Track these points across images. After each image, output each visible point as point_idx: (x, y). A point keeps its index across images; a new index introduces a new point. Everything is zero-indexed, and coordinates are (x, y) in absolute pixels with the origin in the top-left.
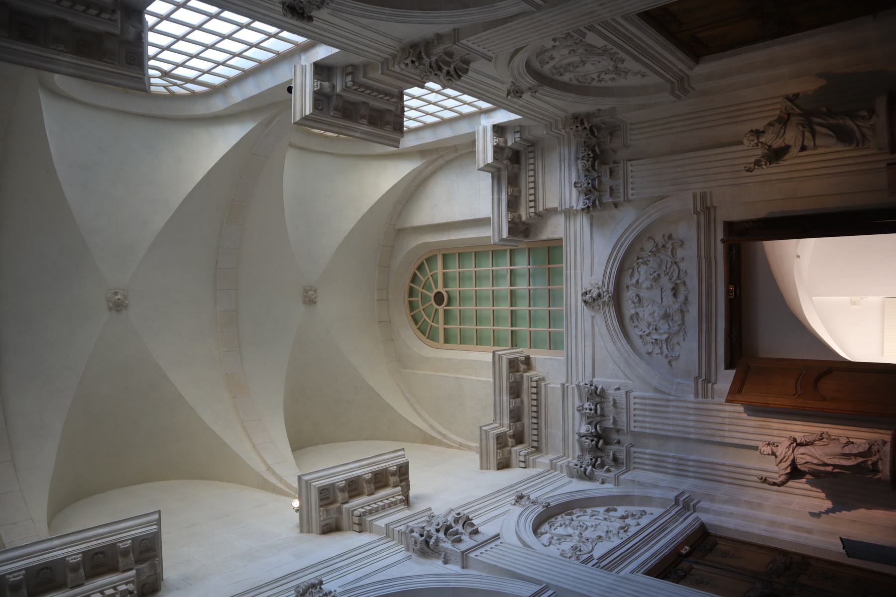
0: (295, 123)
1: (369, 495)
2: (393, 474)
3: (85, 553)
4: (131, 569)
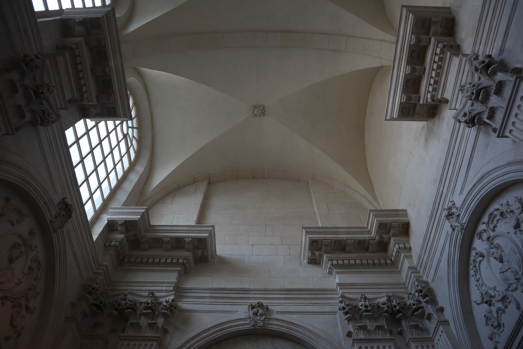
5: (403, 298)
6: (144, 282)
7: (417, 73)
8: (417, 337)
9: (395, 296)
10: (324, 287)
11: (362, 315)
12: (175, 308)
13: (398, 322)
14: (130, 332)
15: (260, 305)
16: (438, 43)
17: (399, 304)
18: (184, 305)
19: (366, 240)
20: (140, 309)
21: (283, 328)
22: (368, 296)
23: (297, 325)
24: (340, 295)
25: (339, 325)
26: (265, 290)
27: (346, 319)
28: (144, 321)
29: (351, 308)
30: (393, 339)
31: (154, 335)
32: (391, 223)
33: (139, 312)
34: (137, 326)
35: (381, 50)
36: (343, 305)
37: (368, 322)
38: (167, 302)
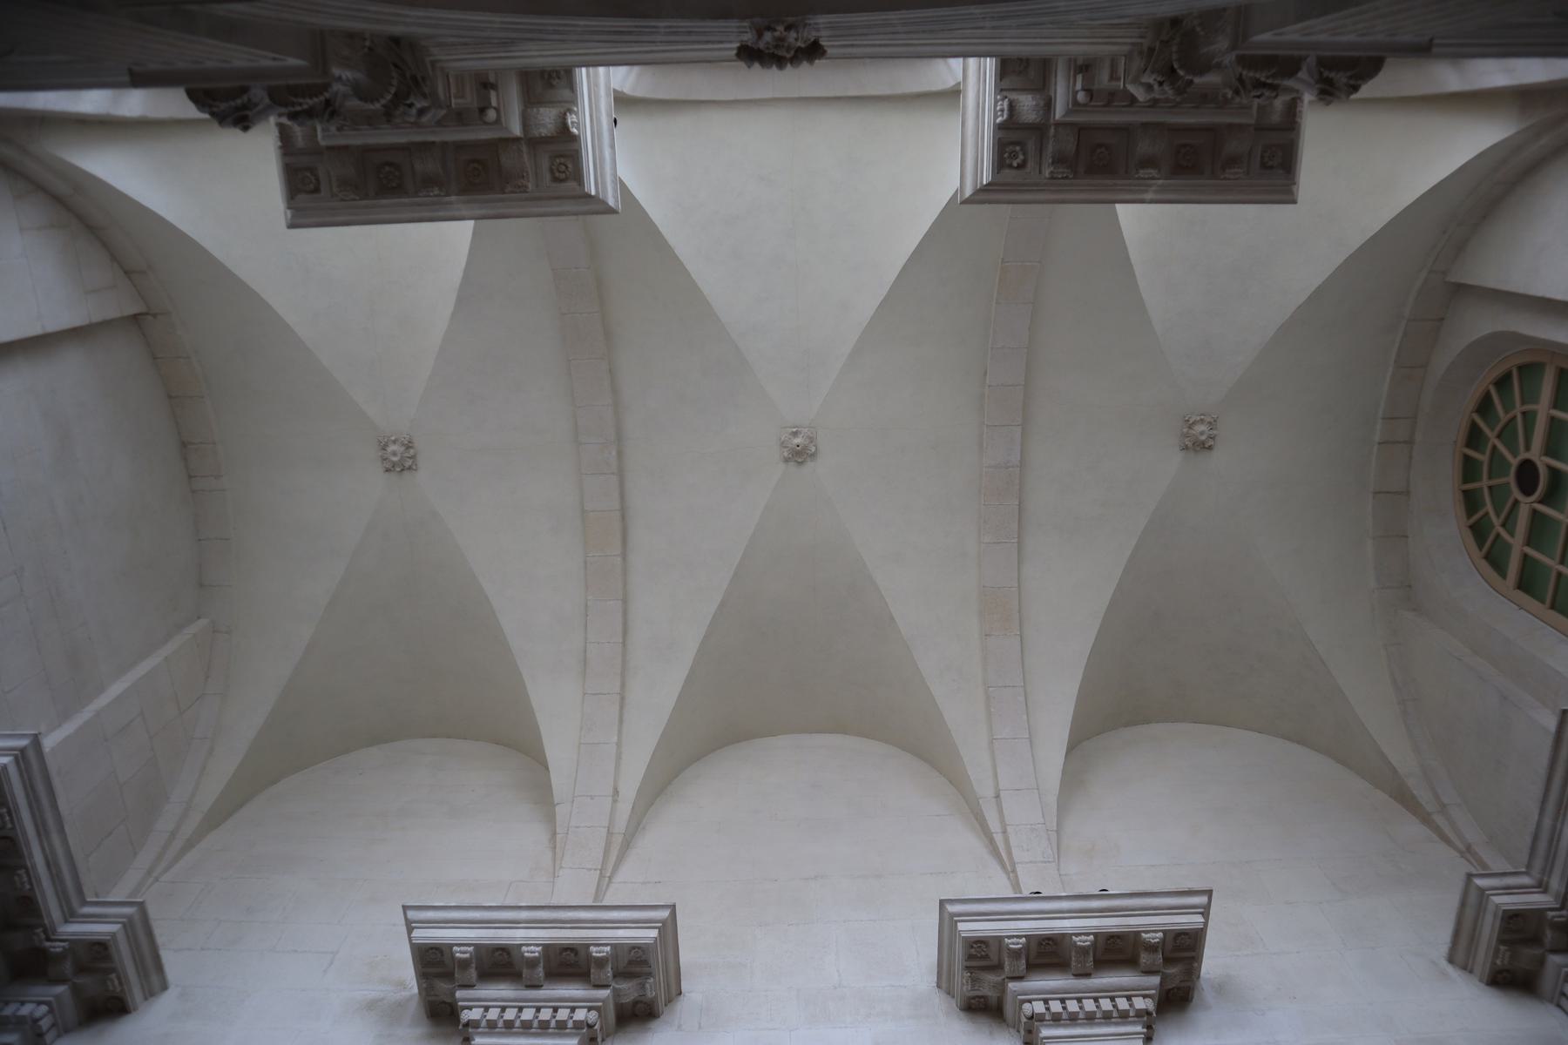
0: (963, 202)
1: (1077, 976)
2: (1152, 948)
3: (547, 948)
4: (605, 986)
7: (525, 972)
16: (597, 1009)
19: (40, 916)
32: (113, 970)
35: (592, 797)
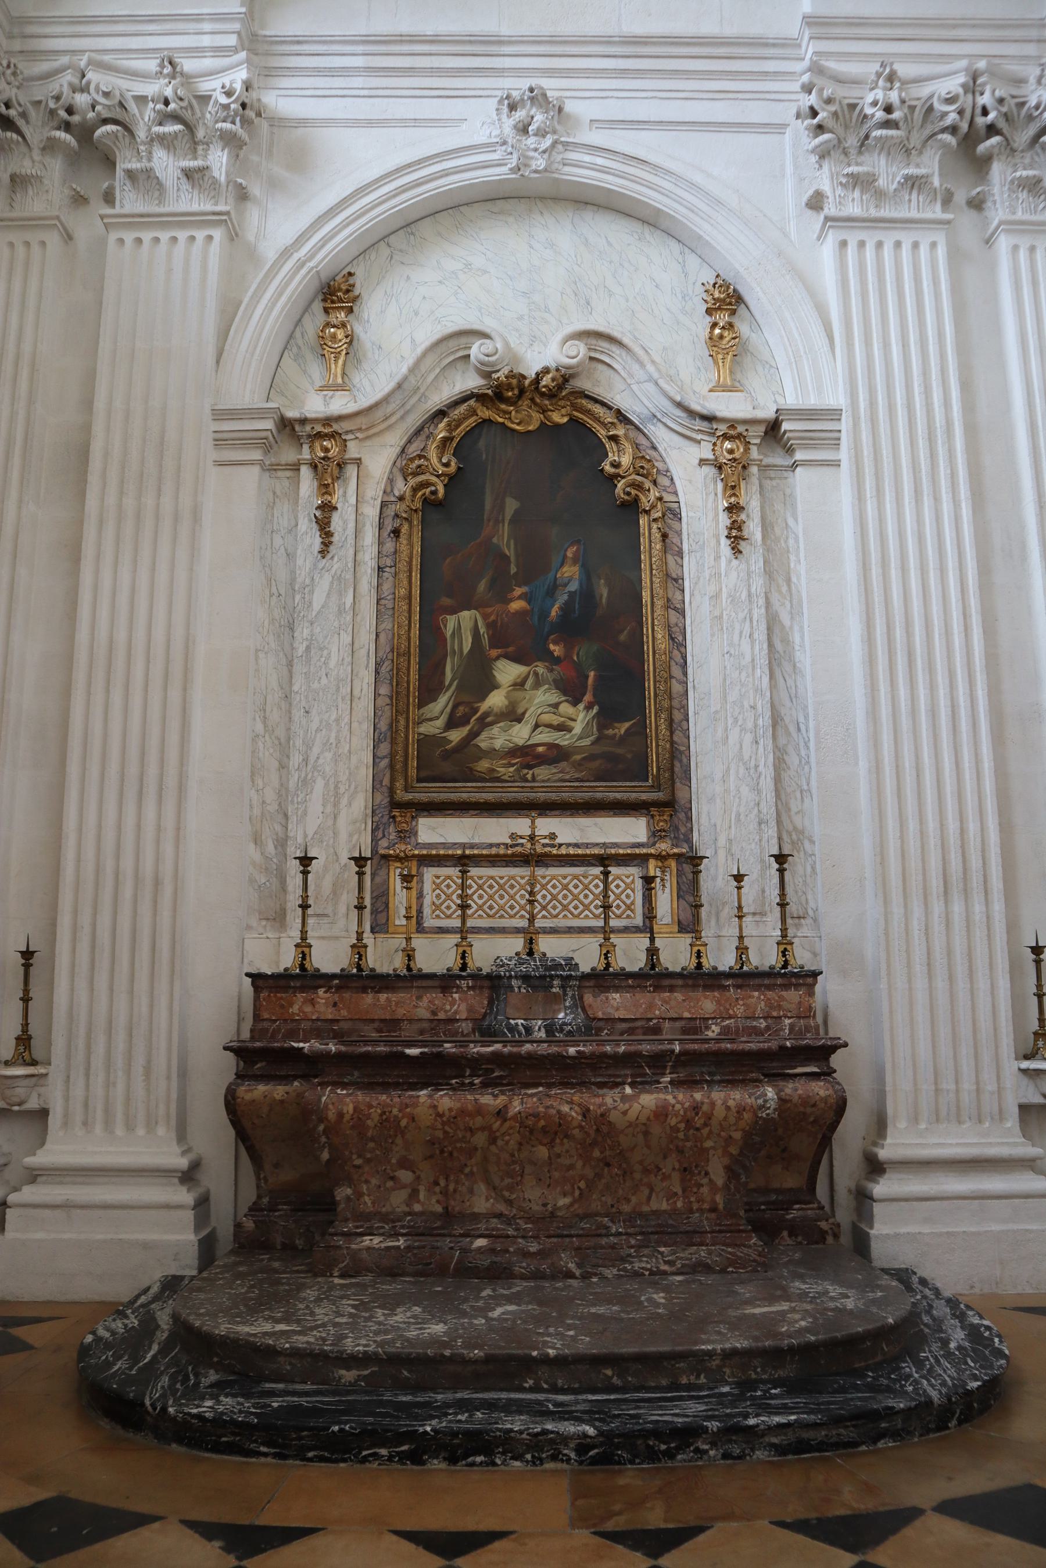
5: (1020, 81)
6: (132, 19)
8: (1027, 217)
9: (992, 72)
10: (755, 30)
11: (867, 137)
12: (259, 114)
13: (981, 165)
14: (130, 201)
15: (537, 97)
17: (1001, 101)
18: (282, 100)
20: (144, 120)
21: (610, 178)
22: (903, 70)
23: (655, 168)
24: (806, 63)
25: (789, 169)
26: (553, 40)
27: (813, 151)
28: (165, 164)
29: (835, 114)
30: (948, 222)
31: (209, 207)
33: (141, 134)
34: (144, 180)
36: (813, 99)
37: (883, 162)
38: (229, 94)
